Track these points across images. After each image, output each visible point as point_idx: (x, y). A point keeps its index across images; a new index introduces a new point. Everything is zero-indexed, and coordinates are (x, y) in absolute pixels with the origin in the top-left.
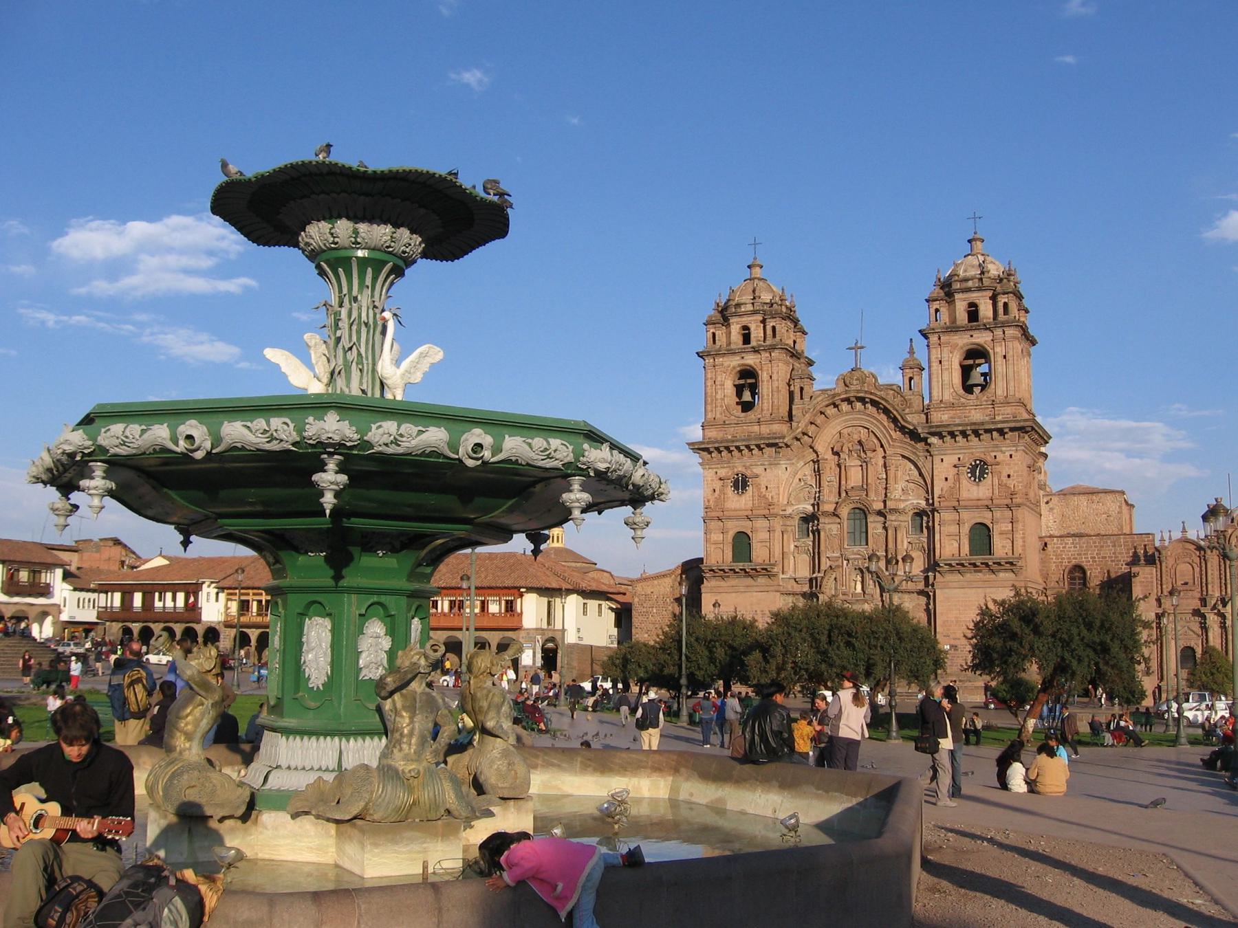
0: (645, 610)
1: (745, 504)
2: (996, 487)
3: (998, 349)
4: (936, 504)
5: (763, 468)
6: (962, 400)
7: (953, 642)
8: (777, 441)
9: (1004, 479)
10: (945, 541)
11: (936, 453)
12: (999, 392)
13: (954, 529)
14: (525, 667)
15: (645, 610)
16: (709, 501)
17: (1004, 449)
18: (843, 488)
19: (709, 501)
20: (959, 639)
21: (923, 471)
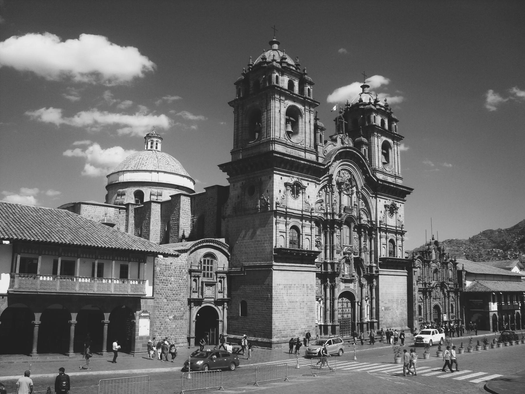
0: (164, 278)
1: (298, 206)
2: (397, 221)
3: (396, 148)
4: (378, 226)
5: (307, 182)
6: (384, 170)
7: (385, 305)
8: (322, 167)
9: (399, 217)
10: (382, 246)
11: (379, 196)
12: (396, 171)
13: (383, 240)
14: (142, 338)
15: (164, 278)
16: (277, 199)
17: (399, 201)
18: (343, 207)
19: (277, 199)
20: (386, 303)
21: (370, 204)
